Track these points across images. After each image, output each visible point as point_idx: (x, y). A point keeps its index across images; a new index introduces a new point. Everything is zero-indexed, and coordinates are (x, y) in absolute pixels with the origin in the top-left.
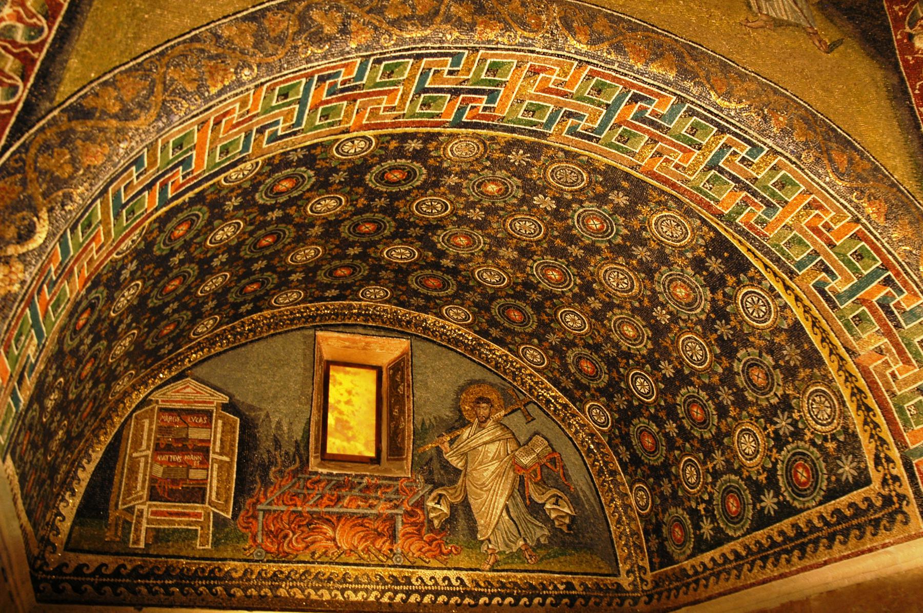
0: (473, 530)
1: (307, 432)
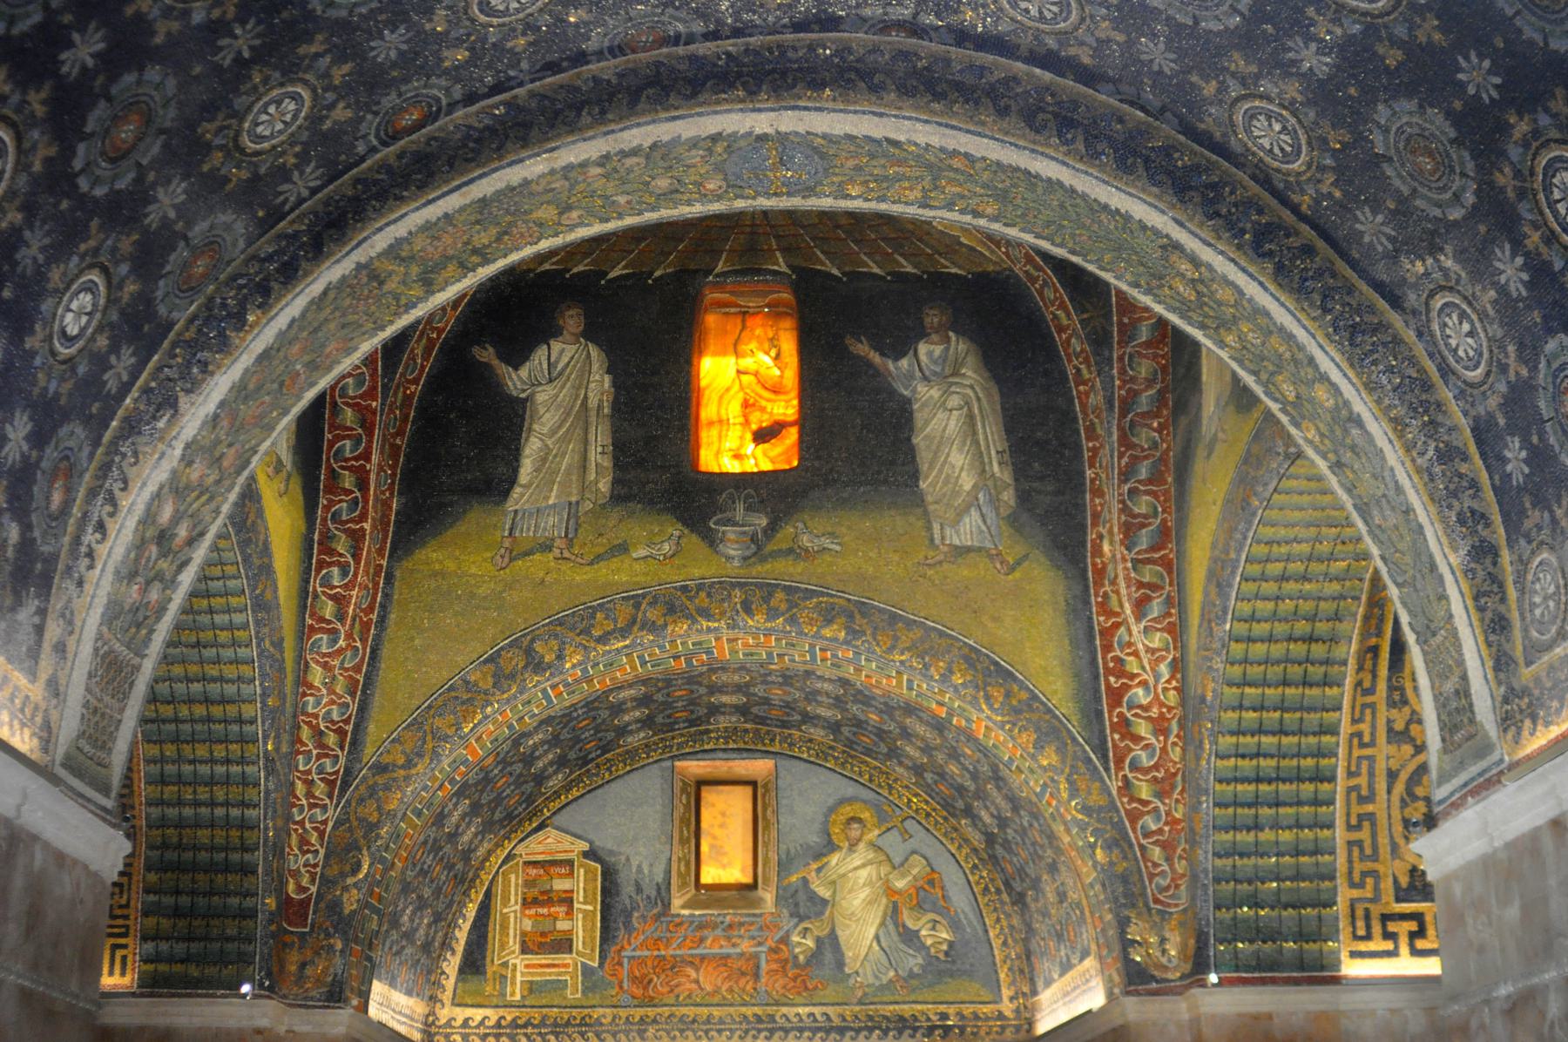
0: (840, 964)
1: (668, 872)
